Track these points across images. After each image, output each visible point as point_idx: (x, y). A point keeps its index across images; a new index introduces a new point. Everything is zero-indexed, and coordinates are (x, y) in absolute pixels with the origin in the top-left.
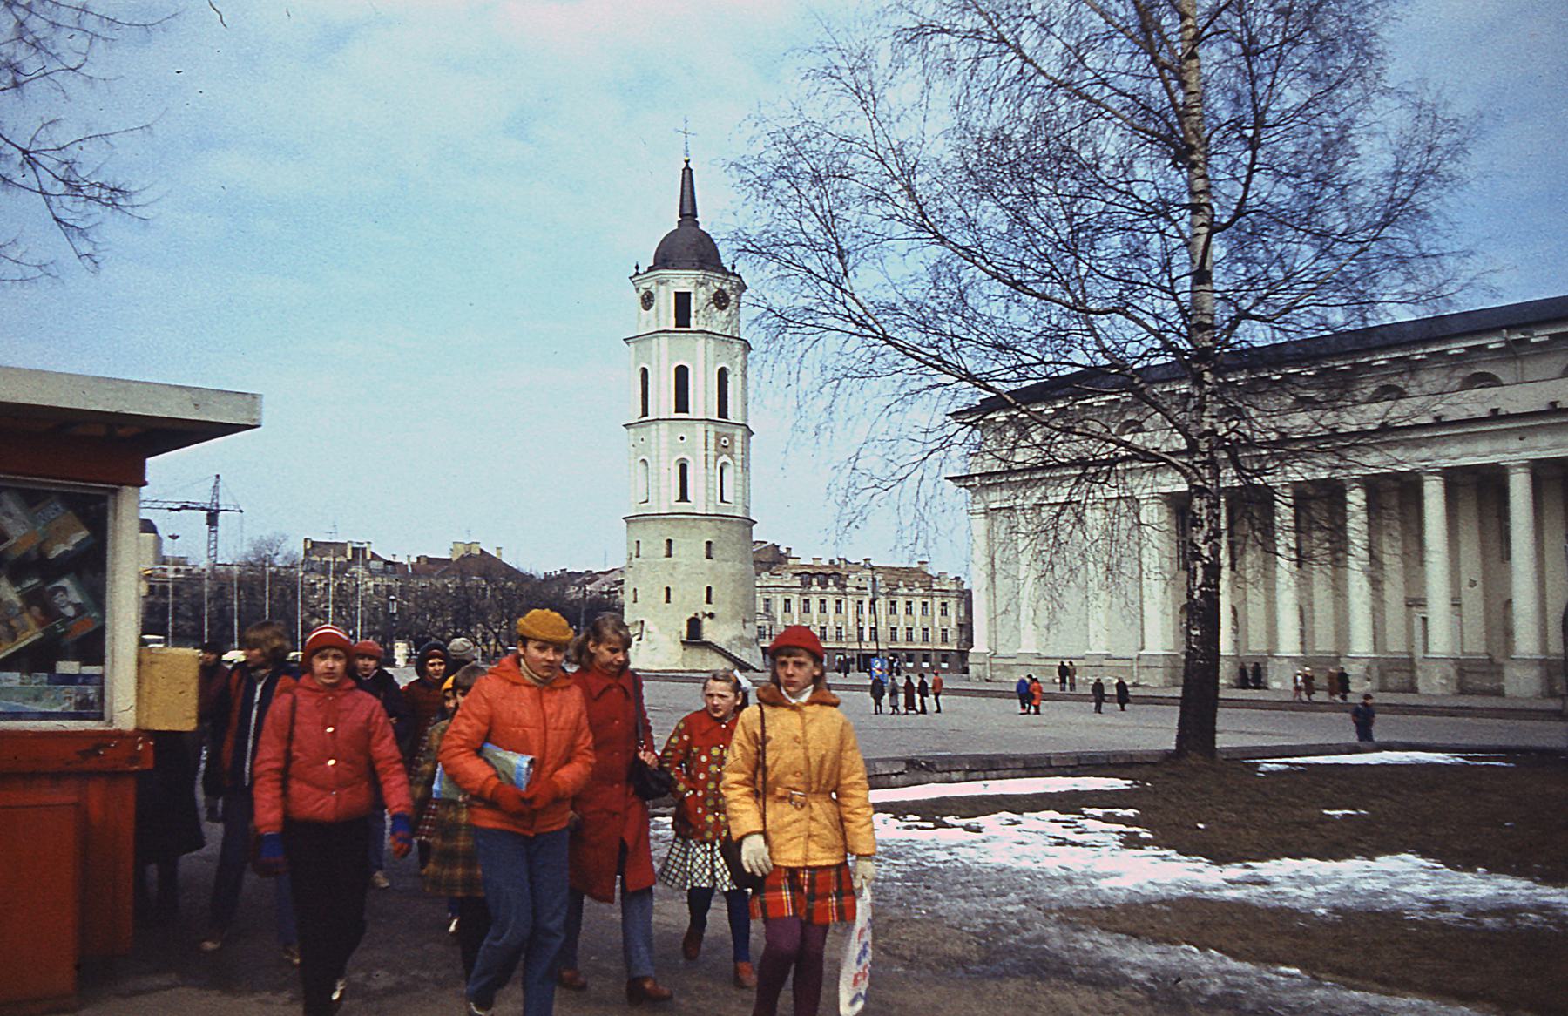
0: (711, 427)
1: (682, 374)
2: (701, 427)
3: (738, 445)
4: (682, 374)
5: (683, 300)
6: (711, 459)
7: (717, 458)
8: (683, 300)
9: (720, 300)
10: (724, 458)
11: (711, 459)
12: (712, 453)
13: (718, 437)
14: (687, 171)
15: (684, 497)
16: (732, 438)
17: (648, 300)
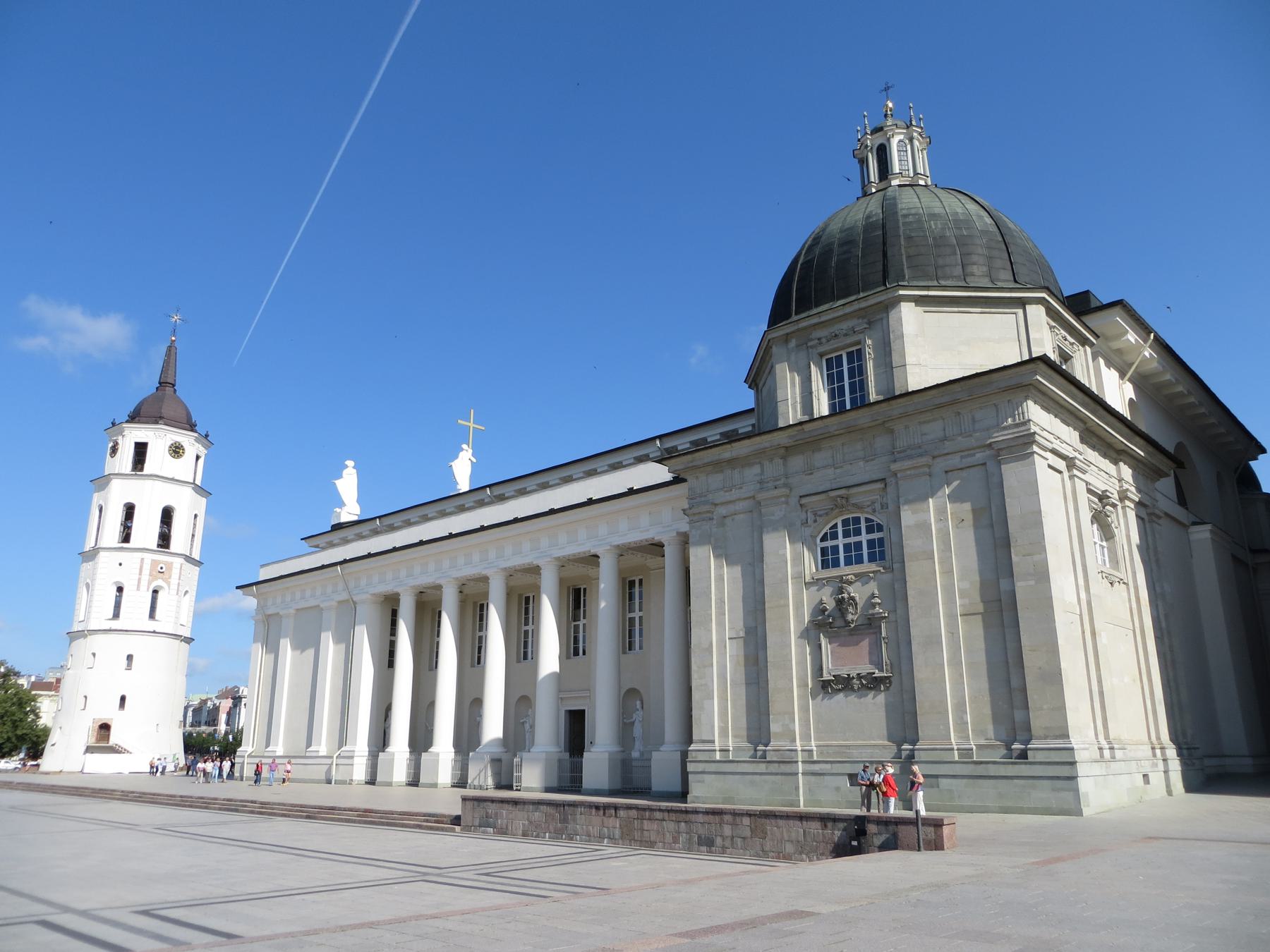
0: (149, 557)
1: (130, 511)
2: (139, 555)
3: (175, 572)
4: (130, 511)
5: (141, 449)
6: (144, 583)
7: (149, 583)
8: (141, 449)
9: (177, 450)
10: (159, 582)
11: (144, 583)
12: (145, 577)
13: (154, 563)
14: (171, 349)
15: (116, 615)
16: (170, 566)
17: (114, 450)
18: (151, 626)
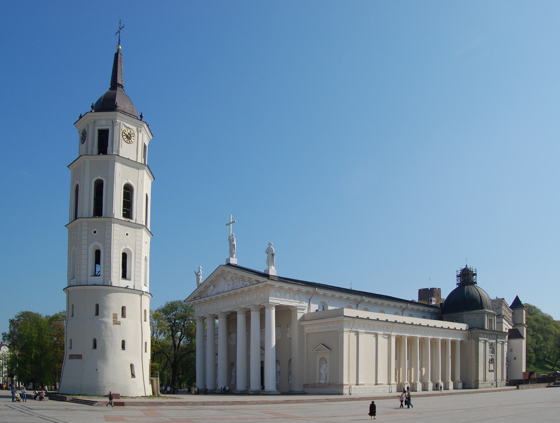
18: (124, 283)
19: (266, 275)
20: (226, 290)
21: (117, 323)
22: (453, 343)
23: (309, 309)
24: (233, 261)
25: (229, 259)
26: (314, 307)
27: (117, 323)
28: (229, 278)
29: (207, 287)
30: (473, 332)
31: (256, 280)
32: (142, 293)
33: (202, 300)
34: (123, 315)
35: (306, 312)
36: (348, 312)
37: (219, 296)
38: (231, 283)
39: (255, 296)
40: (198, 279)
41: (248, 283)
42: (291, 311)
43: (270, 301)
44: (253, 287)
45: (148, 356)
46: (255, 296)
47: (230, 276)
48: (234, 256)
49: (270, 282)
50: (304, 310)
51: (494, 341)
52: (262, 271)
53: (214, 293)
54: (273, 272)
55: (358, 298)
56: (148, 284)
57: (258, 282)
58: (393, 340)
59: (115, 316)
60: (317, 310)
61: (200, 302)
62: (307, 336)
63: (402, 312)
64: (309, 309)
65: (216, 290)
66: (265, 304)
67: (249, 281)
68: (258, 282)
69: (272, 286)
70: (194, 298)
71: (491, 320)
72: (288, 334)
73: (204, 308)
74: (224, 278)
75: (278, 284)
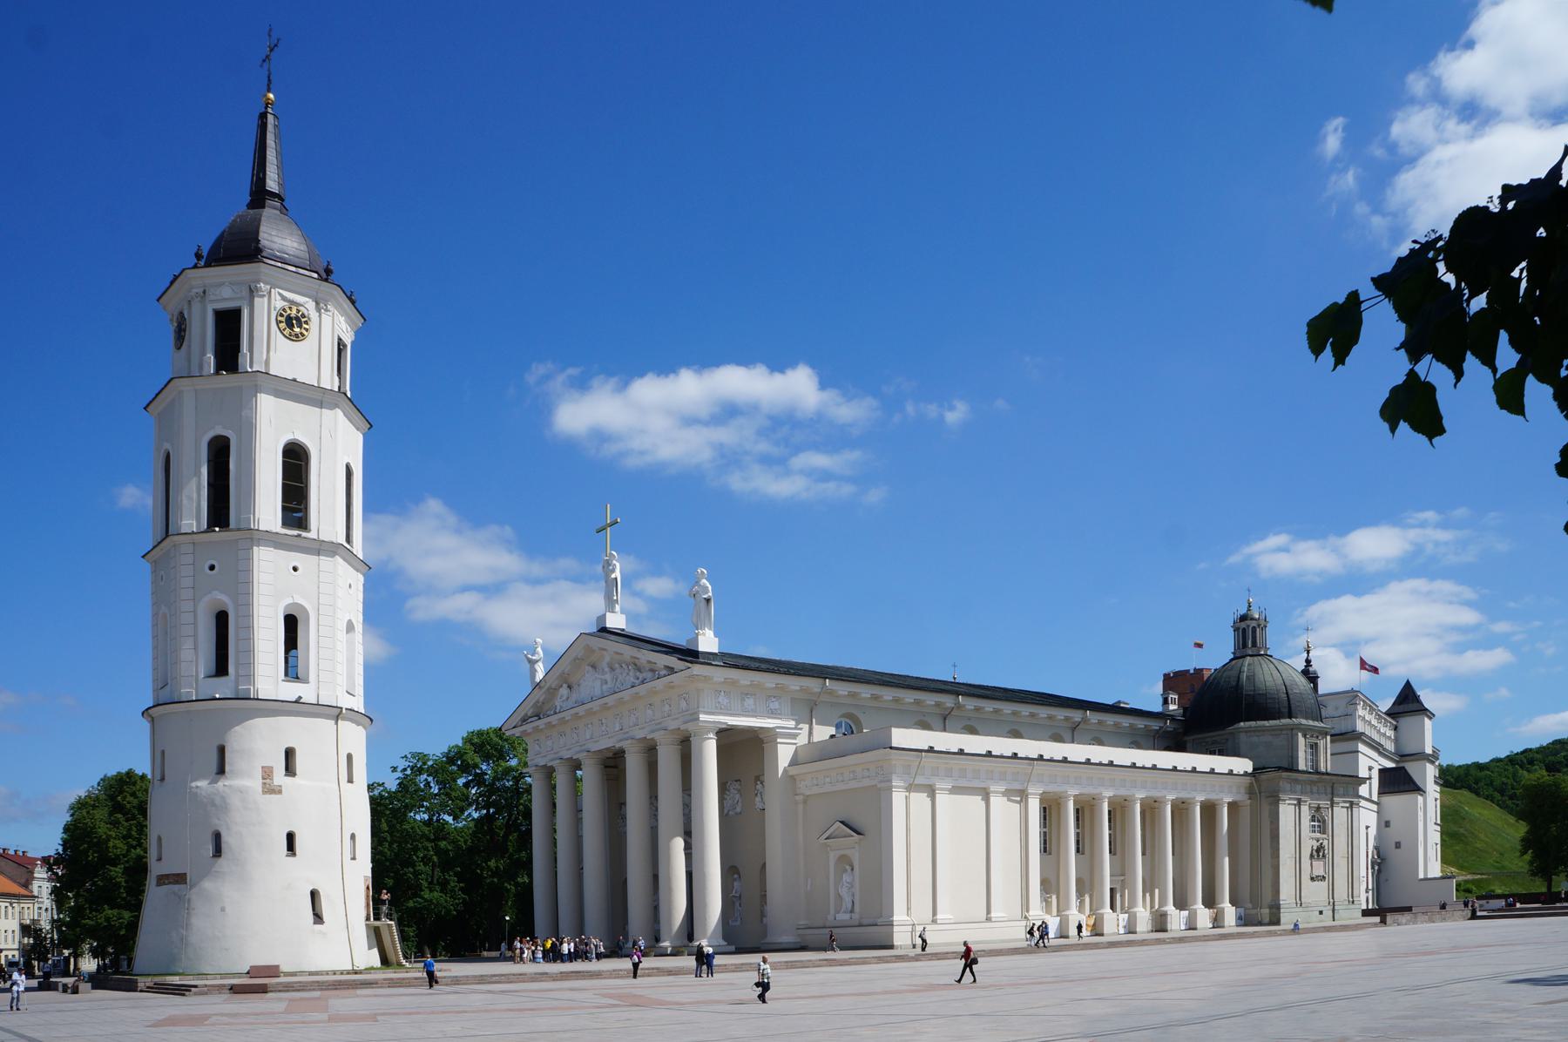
19: (690, 655)
20: (597, 692)
21: (271, 790)
22: (1209, 810)
23: (810, 733)
24: (616, 621)
25: (602, 618)
26: (823, 733)
27: (271, 790)
28: (604, 665)
29: (552, 692)
30: (1264, 777)
31: (667, 667)
32: (337, 714)
33: (541, 723)
34: (290, 770)
35: (802, 740)
36: (904, 737)
37: (581, 710)
38: (608, 677)
39: (667, 708)
40: (533, 672)
41: (649, 675)
42: (762, 741)
43: (703, 717)
44: (659, 684)
45: (363, 868)
46: (667, 708)
47: (607, 659)
48: (618, 608)
49: (697, 669)
50: (794, 736)
51: (1324, 803)
52: (680, 640)
53: (570, 703)
54: (708, 642)
55: (948, 701)
56: (359, 690)
57: (671, 670)
58: (1034, 806)
59: (267, 773)
60: (832, 736)
61: (536, 729)
62: (805, 802)
63: (1073, 734)
64: (810, 733)
65: (574, 696)
66: (690, 727)
67: (652, 671)
68: (671, 670)
69: (707, 679)
70: (524, 720)
71: (1314, 747)
72: (758, 799)
73: (549, 743)
74: (594, 667)
75: (720, 674)
